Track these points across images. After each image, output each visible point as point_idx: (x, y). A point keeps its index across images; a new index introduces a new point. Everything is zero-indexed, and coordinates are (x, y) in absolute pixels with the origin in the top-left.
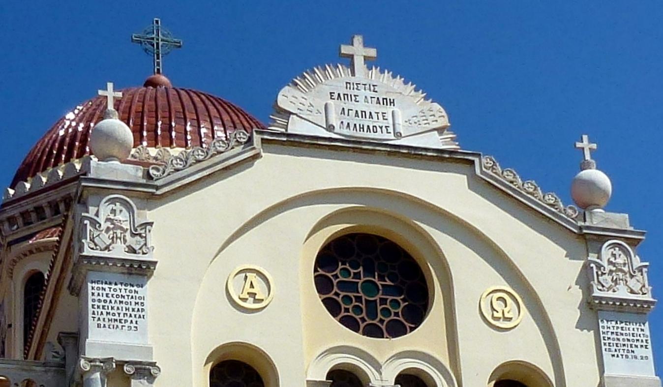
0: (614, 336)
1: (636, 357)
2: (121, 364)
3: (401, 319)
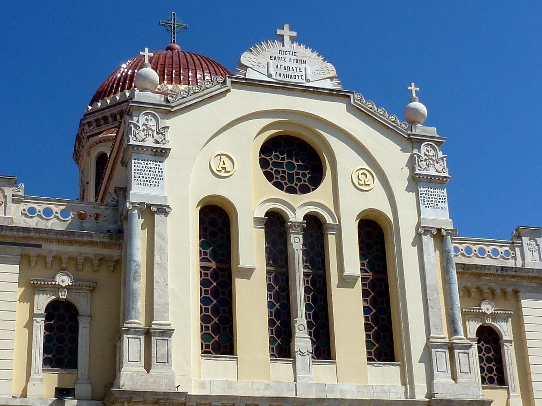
0: (427, 196)
1: (439, 208)
2: (149, 206)
3: (307, 184)
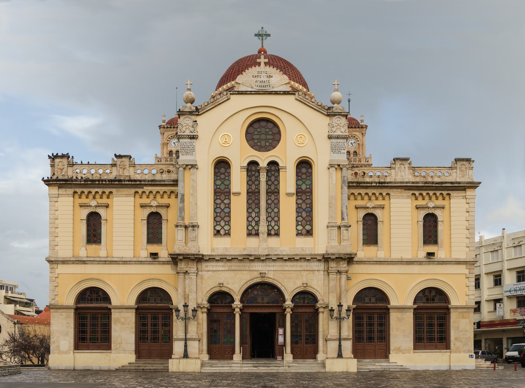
0: (335, 147)
1: (341, 153)
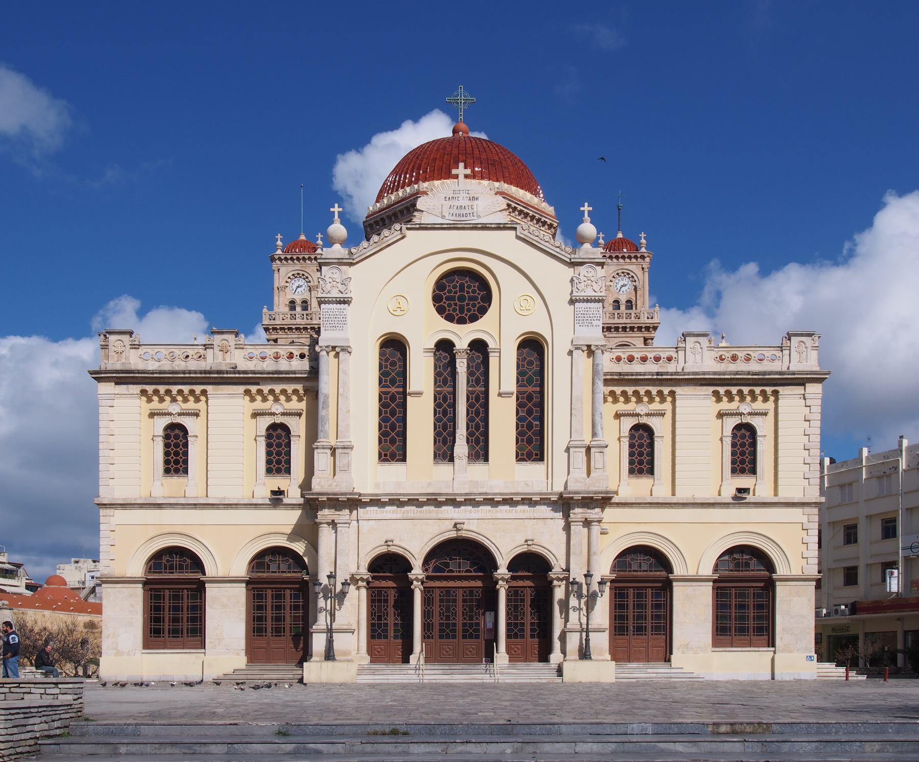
0: (583, 316)
1: (593, 326)
